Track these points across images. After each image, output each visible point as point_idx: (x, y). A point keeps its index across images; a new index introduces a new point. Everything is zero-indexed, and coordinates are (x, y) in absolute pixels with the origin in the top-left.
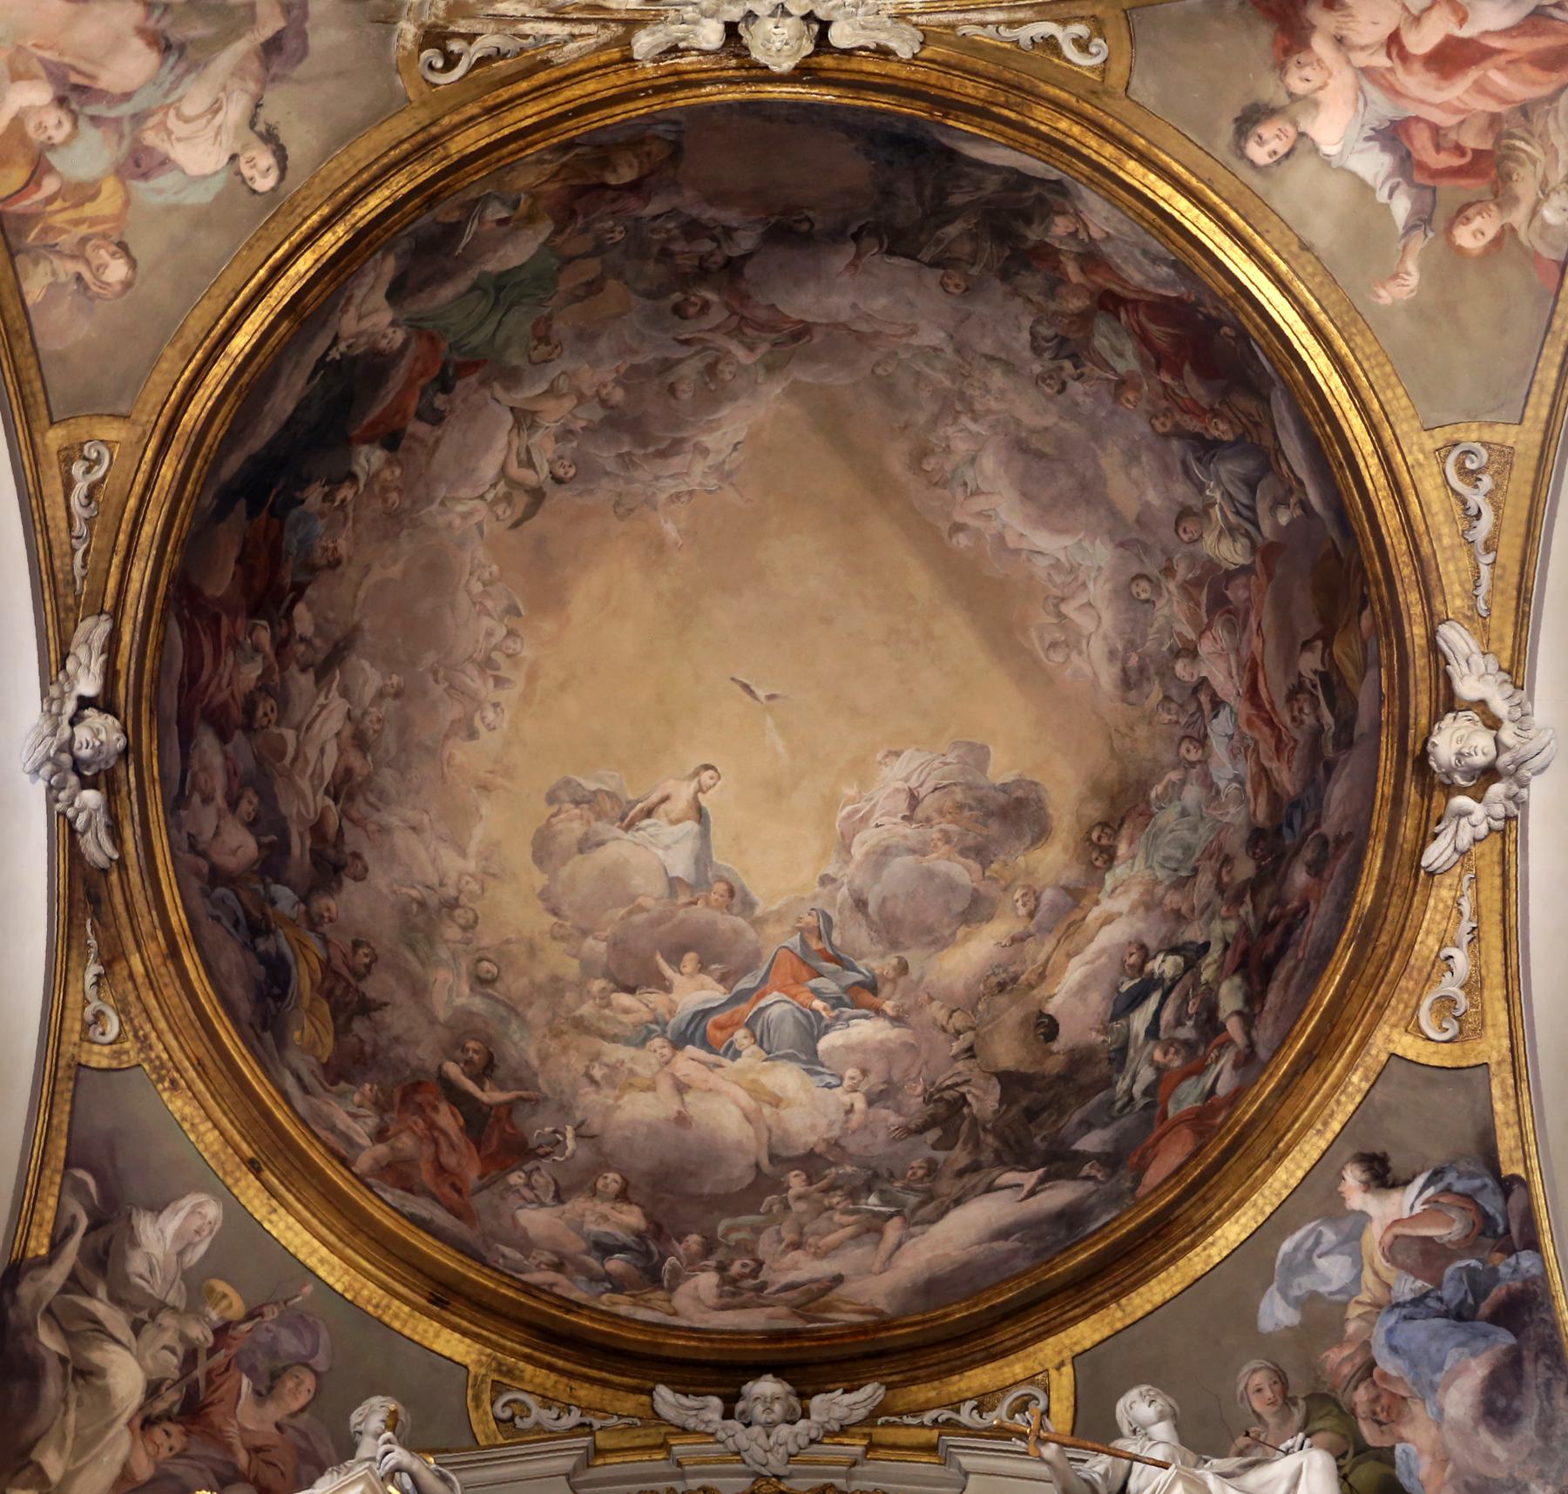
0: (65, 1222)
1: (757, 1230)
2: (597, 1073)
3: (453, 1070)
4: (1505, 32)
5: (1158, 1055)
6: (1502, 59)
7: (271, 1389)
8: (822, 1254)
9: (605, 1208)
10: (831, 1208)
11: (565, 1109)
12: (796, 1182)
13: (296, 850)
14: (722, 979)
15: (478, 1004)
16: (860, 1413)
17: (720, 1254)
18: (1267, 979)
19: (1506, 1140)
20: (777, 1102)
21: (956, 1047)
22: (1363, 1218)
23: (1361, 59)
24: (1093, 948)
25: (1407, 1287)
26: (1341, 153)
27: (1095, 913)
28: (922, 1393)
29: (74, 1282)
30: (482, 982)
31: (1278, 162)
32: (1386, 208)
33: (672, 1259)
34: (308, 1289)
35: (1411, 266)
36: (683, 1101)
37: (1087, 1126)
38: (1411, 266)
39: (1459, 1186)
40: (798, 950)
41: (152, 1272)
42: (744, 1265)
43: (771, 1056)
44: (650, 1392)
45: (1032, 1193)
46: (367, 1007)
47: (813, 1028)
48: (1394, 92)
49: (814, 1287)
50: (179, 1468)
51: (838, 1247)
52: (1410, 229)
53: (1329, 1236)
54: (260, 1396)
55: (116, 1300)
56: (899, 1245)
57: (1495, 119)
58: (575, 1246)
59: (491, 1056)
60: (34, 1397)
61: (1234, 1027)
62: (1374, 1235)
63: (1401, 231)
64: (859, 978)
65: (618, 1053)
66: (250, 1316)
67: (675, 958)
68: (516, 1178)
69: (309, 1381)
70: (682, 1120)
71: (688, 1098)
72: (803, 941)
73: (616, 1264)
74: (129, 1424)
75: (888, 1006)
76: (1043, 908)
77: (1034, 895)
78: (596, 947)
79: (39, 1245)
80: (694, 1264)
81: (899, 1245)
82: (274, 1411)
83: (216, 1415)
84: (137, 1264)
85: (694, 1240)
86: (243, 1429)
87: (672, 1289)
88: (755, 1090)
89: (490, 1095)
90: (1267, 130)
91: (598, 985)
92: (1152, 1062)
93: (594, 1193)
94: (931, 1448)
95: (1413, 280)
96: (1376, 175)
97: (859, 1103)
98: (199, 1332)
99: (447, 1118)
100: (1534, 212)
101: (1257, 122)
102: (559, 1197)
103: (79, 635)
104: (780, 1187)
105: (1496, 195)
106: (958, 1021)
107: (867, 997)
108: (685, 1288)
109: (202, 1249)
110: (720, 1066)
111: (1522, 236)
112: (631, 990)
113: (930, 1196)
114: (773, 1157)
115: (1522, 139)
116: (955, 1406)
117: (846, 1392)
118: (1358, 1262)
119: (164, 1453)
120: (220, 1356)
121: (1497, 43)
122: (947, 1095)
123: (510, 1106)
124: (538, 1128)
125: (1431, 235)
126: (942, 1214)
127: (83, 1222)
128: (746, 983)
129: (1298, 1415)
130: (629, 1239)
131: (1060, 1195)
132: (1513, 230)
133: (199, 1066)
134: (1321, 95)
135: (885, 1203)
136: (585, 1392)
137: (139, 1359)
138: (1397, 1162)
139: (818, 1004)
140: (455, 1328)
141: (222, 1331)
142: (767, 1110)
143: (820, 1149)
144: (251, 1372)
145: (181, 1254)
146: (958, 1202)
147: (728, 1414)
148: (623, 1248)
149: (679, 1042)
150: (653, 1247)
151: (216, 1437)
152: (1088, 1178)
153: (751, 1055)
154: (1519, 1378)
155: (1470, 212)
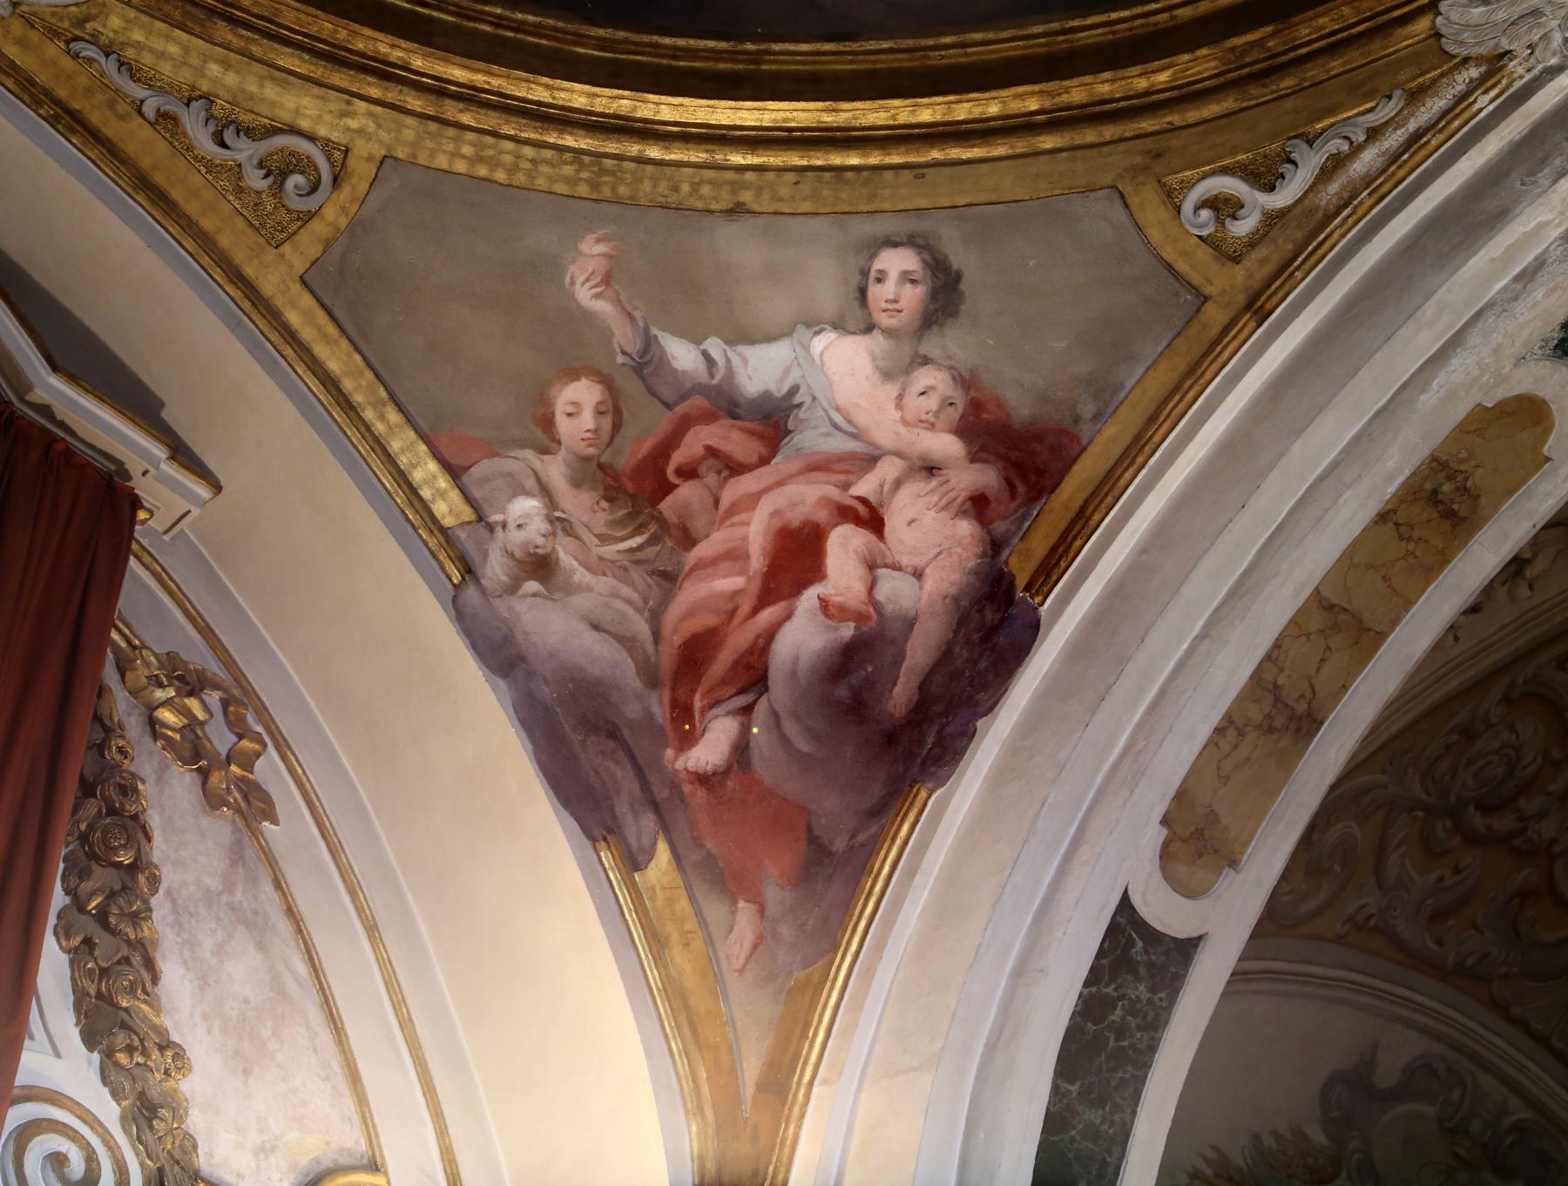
4: (770, 634)
6: (746, 606)
23: (889, 469)
26: (807, 349)
31: (865, 273)
32: (697, 340)
35: (603, 307)
38: (603, 307)
48: (819, 466)
52: (649, 342)
57: (688, 540)
63: (654, 331)
90: (913, 297)
95: (584, 295)
96: (745, 361)
100: (545, 492)
101: (934, 294)
105: (601, 466)
111: (528, 454)
115: (640, 548)
121: (767, 615)
125: (620, 359)
132: (545, 451)
134: (892, 390)
155: (607, 423)
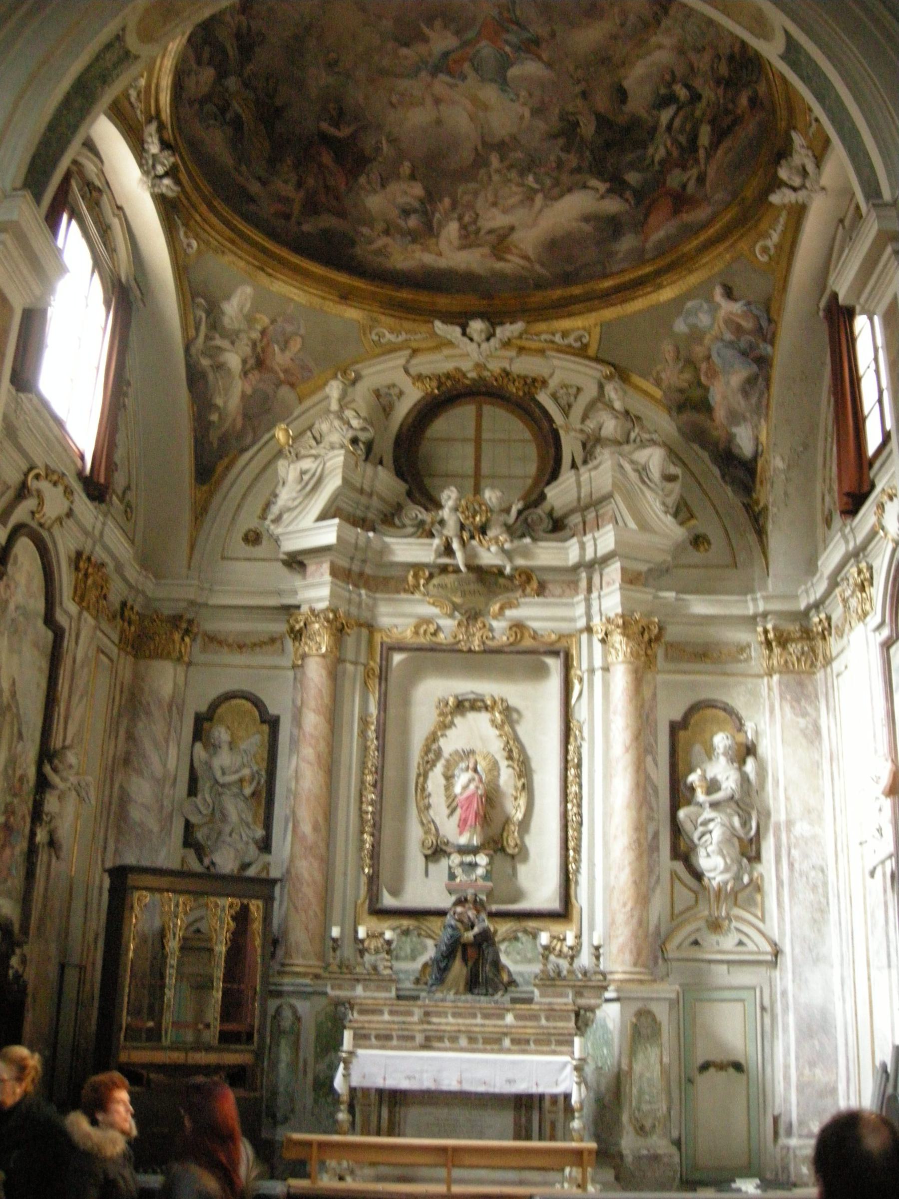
0: (197, 318)
1: (476, 194)
2: (394, 99)
3: (324, 126)
5: (669, 143)
7: (286, 347)
8: (505, 212)
9: (404, 186)
10: (510, 181)
11: (379, 127)
12: (495, 160)
13: (231, 53)
14: (458, 33)
15: (331, 80)
16: (516, 334)
17: (459, 210)
18: (719, 142)
19: (774, 306)
20: (486, 107)
21: (578, 89)
22: (719, 306)
24: (649, 60)
25: (728, 336)
27: (654, 40)
28: (542, 326)
29: (208, 338)
30: (331, 65)
33: (437, 215)
34: (292, 306)
36: (439, 111)
37: (632, 166)
39: (756, 312)
40: (497, 17)
41: (232, 321)
42: (470, 217)
43: (483, 80)
44: (432, 323)
45: (603, 197)
46: (278, 112)
47: (505, 63)
49: (501, 232)
50: (261, 385)
51: (513, 207)
53: (705, 306)
54: (282, 350)
55: (223, 336)
56: (541, 211)
58: (394, 213)
59: (341, 108)
60: (206, 383)
61: (702, 153)
62: (722, 313)
64: (529, 35)
65: (404, 84)
66: (273, 321)
67: (430, 21)
68: (362, 180)
69: (299, 340)
70: (439, 122)
71: (442, 107)
72: (500, 13)
73: (413, 222)
74: (240, 377)
75: (545, 56)
76: (629, 23)
77: (624, 13)
78: (387, 24)
79: (192, 333)
80: (447, 217)
81: (541, 211)
82: (288, 354)
83: (268, 362)
84: (226, 321)
85: (447, 201)
86: (278, 364)
87: (437, 236)
88: (475, 100)
89: (344, 132)
91: (390, 45)
92: (666, 146)
93: (398, 177)
94: (542, 352)
97: (527, 114)
98: (255, 335)
99: (327, 158)
102: (383, 186)
103: (146, 134)
104: (487, 164)
106: (580, 73)
107: (533, 47)
108: (444, 233)
109: (248, 305)
110: (456, 86)
112: (407, 45)
113: (557, 183)
114: (484, 143)
116: (554, 334)
117: (511, 323)
118: (714, 319)
119: (254, 382)
120: (265, 340)
122: (571, 118)
123: (354, 136)
124: (368, 142)
126: (561, 195)
127: (204, 316)
128: (470, 35)
129: (681, 364)
130: (416, 204)
131: (613, 206)
133: (232, 242)
135: (537, 181)
136: (407, 325)
137: (237, 353)
138: (736, 292)
139: (508, 49)
140: (351, 306)
141: (263, 332)
142: (481, 114)
143: (507, 139)
144: (278, 343)
145: (241, 310)
146: (570, 190)
147: (464, 334)
148: (415, 211)
149: (436, 71)
150: (428, 207)
151: (271, 370)
152: (627, 200)
153: (471, 75)
154: (756, 383)
